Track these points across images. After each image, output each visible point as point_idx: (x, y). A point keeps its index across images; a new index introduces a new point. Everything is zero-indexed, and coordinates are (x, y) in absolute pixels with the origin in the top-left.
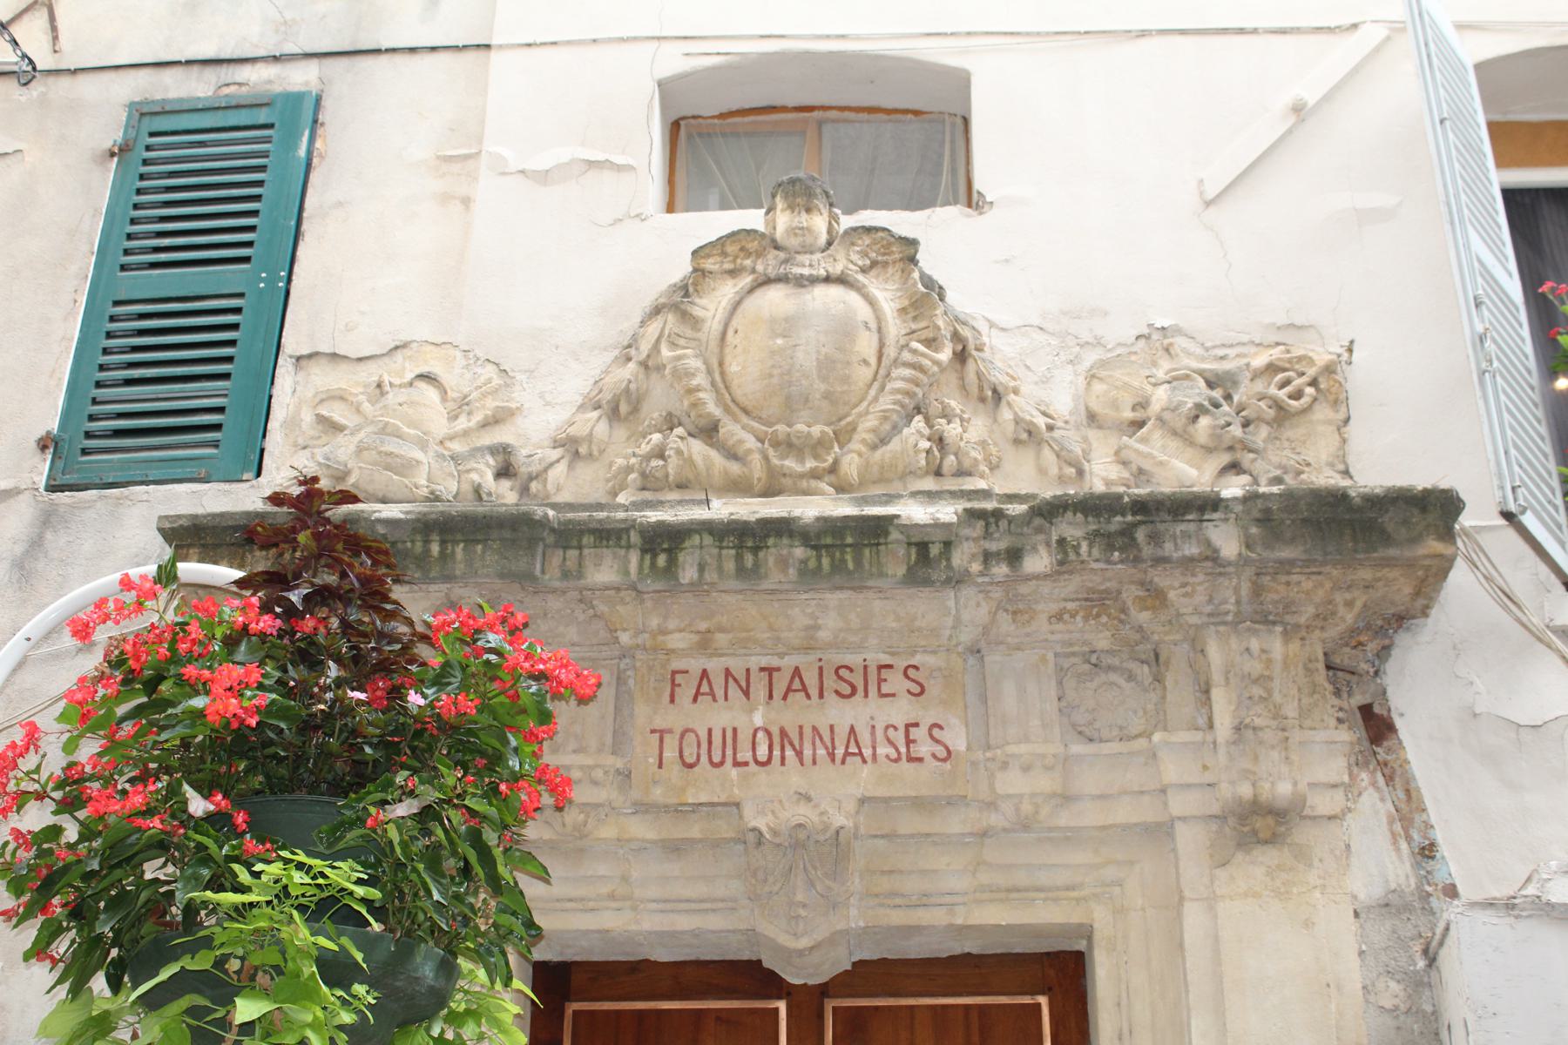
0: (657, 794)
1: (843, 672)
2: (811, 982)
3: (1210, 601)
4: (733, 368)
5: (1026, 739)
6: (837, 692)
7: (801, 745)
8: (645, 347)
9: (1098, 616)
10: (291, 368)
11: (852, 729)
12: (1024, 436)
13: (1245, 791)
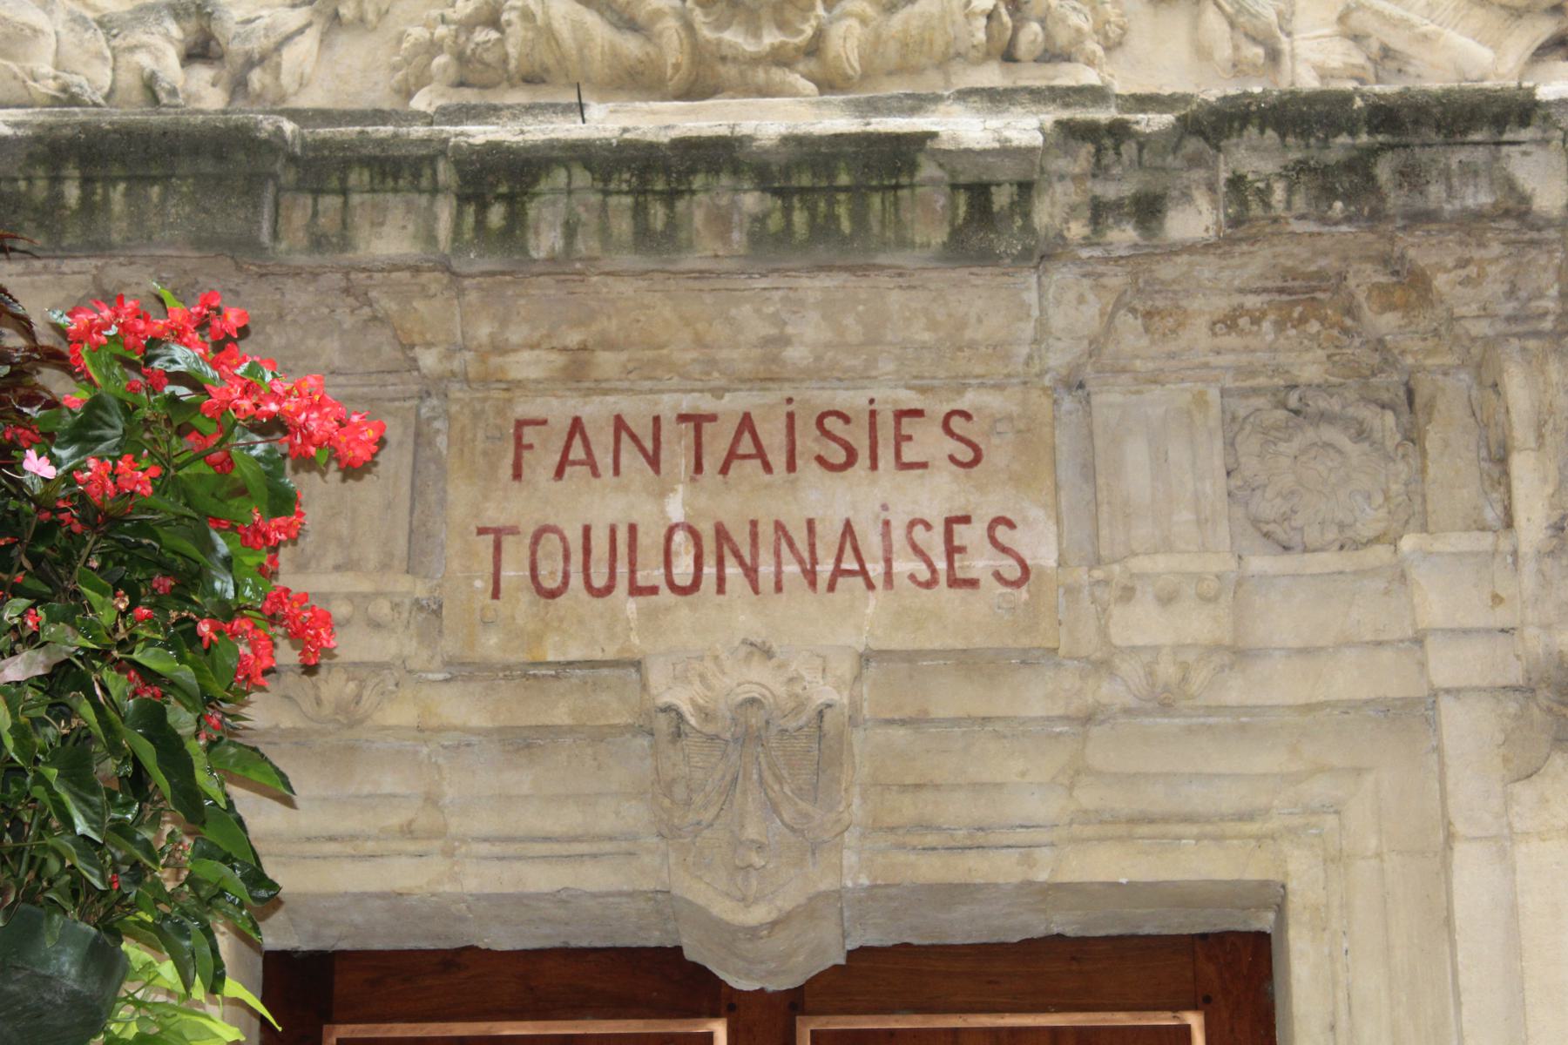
0: (491, 645)
1: (832, 424)
2: (772, 986)
3: (1512, 293)
6: (820, 460)
9: (1303, 320)
11: (848, 528)
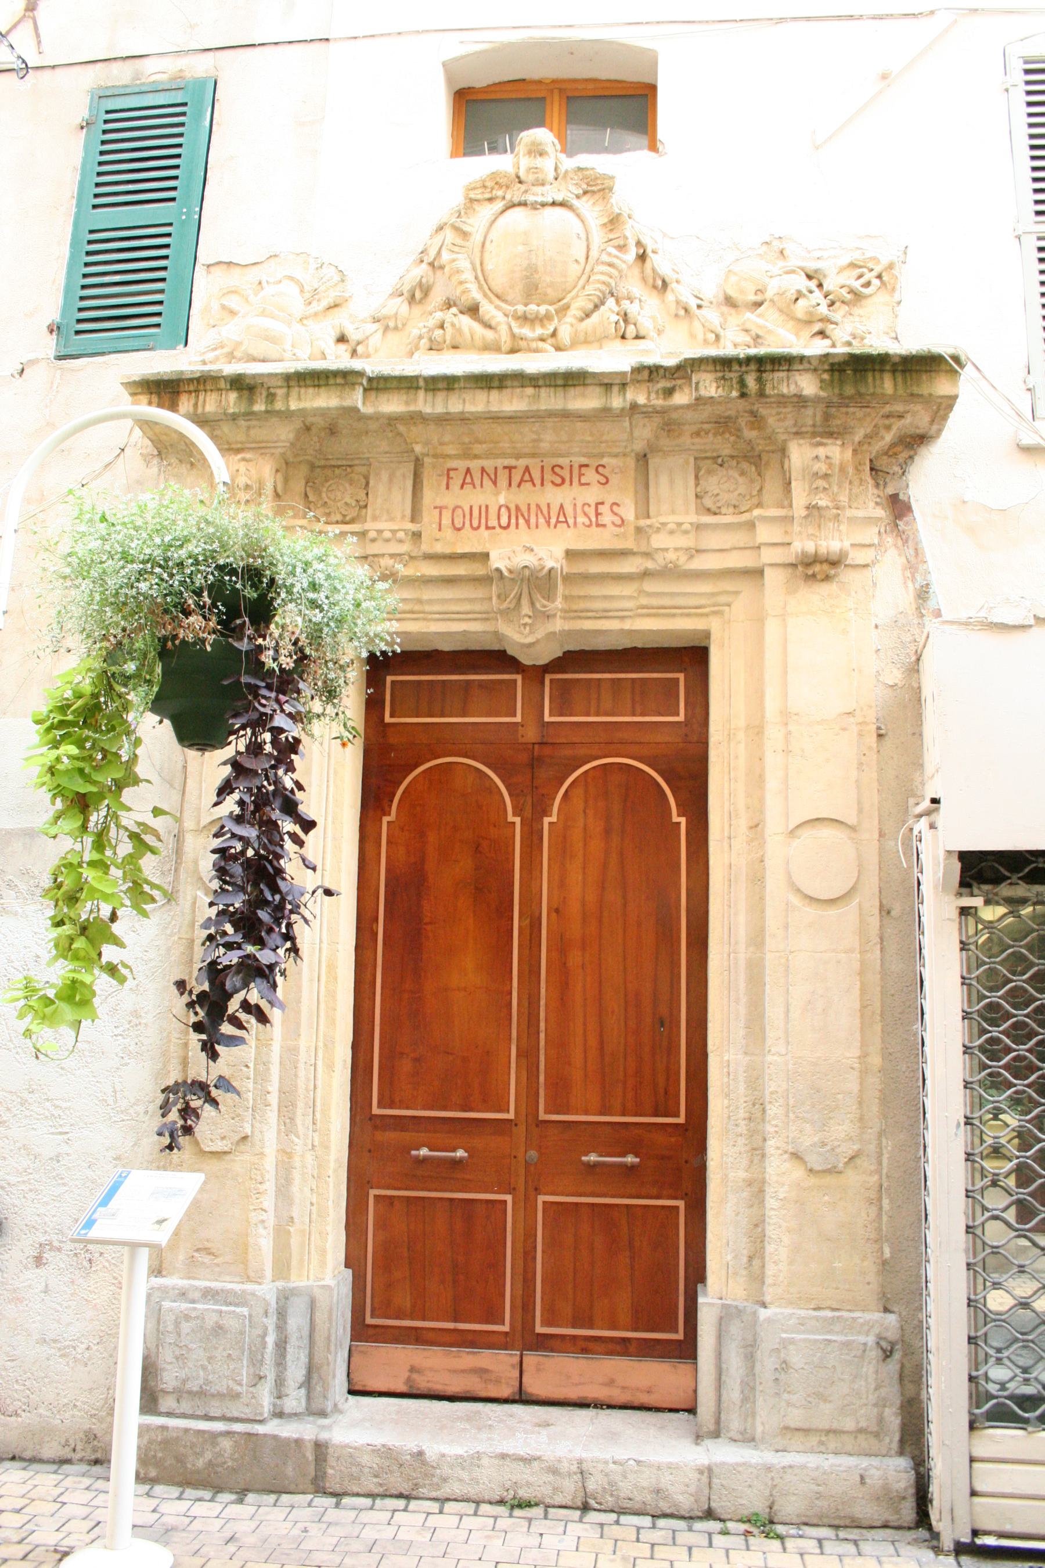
0: (439, 548)
1: (557, 469)
2: (537, 664)
3: (795, 425)
4: (489, 266)
5: (673, 512)
6: (553, 482)
7: (529, 516)
8: (432, 253)
9: (723, 433)
10: (204, 273)
11: (562, 506)
12: (682, 312)
13: (810, 547)
